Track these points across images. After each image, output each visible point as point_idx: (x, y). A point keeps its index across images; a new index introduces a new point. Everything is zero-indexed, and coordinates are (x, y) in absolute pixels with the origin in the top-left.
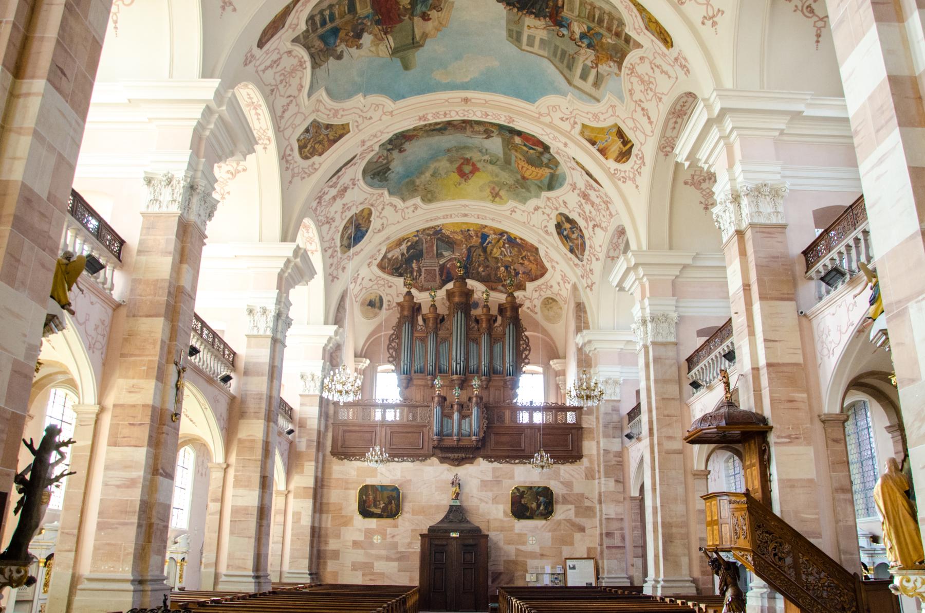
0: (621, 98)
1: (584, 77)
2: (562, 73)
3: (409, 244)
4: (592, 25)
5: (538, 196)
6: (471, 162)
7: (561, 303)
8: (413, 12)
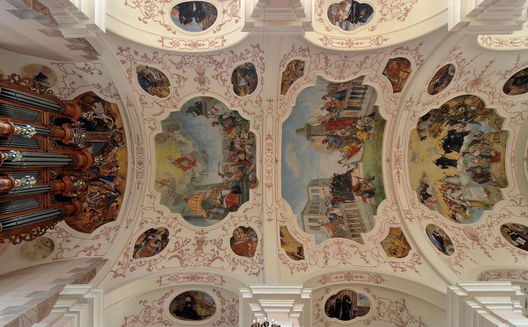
0: (318, 242)
1: (310, 220)
2: (305, 209)
3: (106, 121)
4: (345, 217)
5: (173, 211)
6: (191, 166)
7: (53, 255)
8: (330, 136)
